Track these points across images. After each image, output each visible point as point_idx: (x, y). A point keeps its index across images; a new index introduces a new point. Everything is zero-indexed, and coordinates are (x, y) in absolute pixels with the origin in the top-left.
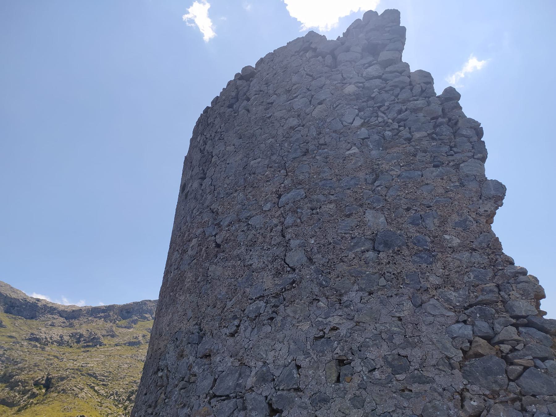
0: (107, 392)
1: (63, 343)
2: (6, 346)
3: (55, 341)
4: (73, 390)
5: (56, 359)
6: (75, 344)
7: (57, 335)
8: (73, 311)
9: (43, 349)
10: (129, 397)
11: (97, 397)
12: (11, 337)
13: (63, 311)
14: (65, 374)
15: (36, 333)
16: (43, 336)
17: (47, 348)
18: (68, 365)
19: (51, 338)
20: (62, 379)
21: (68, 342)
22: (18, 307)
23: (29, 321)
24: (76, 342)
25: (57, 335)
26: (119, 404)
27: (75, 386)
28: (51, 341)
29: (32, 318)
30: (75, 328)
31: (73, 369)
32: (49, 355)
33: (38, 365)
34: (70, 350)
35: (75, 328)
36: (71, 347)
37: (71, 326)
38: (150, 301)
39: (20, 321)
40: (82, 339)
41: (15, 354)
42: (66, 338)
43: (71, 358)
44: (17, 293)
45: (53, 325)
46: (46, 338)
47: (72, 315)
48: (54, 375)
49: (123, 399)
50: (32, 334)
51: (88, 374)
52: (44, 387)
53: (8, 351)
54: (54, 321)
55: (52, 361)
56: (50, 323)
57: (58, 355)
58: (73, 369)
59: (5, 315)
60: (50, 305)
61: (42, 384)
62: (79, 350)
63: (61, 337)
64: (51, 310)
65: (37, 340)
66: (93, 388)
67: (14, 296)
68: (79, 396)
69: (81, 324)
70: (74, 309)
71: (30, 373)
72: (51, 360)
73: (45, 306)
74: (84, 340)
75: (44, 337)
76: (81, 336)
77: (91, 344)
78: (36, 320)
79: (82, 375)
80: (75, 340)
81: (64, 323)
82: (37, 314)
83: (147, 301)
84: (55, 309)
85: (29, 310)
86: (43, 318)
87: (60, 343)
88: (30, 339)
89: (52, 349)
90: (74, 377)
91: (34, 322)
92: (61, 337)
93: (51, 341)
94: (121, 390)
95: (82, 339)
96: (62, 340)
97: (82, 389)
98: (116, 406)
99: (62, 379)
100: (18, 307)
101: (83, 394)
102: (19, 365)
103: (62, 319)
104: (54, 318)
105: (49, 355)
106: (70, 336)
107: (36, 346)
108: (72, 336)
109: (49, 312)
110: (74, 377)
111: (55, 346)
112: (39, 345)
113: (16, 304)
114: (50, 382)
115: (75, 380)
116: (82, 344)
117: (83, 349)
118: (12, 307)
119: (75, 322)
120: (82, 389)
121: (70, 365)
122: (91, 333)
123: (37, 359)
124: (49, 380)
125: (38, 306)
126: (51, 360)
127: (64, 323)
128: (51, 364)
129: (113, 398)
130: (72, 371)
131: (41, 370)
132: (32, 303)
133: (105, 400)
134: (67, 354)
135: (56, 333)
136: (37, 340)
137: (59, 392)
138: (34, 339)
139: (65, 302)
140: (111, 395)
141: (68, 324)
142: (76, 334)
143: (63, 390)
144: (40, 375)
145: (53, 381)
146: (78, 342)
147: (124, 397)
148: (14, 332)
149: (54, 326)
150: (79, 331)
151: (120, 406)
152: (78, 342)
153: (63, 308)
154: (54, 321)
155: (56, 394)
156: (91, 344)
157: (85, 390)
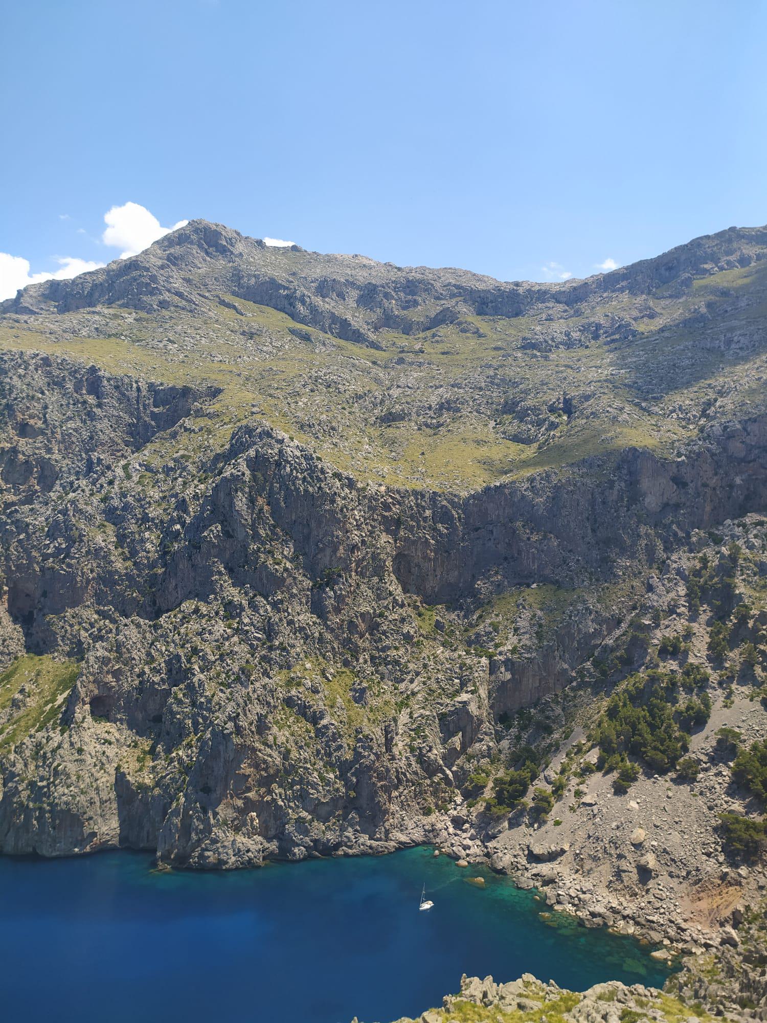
0: (663, 409)
1: (574, 344)
2: (495, 363)
3: (561, 343)
4: (608, 411)
5: (569, 370)
6: (593, 342)
7: (561, 333)
8: (575, 289)
9: (546, 358)
10: (704, 411)
11: (649, 418)
12: (497, 349)
13: (560, 293)
14: (589, 390)
15: (529, 336)
16: (541, 338)
17: (553, 356)
18: (590, 376)
19: (553, 339)
20: (587, 398)
21: (580, 341)
22: (492, 302)
23: (514, 321)
24: (593, 338)
25: (561, 333)
26: (688, 424)
27: (610, 406)
28: (554, 344)
29: (517, 315)
30: (585, 315)
31: (599, 381)
32: (557, 366)
33: (547, 384)
34: (587, 352)
35: (585, 315)
36: (587, 347)
37: (578, 313)
38: (708, 237)
39: (502, 323)
40: (602, 331)
41: (510, 373)
42: (575, 335)
43: (592, 364)
44: (485, 282)
45: (549, 319)
46: (546, 341)
47: (574, 296)
48: (573, 394)
49: (694, 416)
50: (524, 339)
51: (625, 385)
52: (565, 413)
53: (500, 370)
54: (550, 312)
55: (565, 374)
56: (544, 316)
57: (571, 363)
58: (599, 381)
59: (480, 318)
60: (536, 288)
61: (560, 409)
62: (601, 350)
63: (567, 334)
64: (541, 295)
65: (534, 346)
66: (636, 405)
67: (481, 286)
68: (620, 419)
69: (593, 308)
70: (574, 285)
71: (539, 396)
72: (562, 372)
73: (529, 291)
74: (605, 333)
75: (542, 340)
76: (598, 326)
77: (617, 337)
78: (523, 316)
79: (616, 387)
80: (590, 336)
81: (565, 311)
82: (522, 307)
83: (701, 238)
84: (545, 292)
85: (504, 303)
86: (532, 312)
87: (569, 344)
88: (523, 348)
89: (560, 356)
90: (604, 393)
91: (522, 320)
92: (567, 334)
93: (554, 344)
94: (687, 402)
95: (602, 331)
96: (569, 339)
97: (621, 409)
98: (684, 427)
99: (587, 398)
100: (492, 302)
101: (625, 416)
102: (521, 386)
103: (561, 307)
104: (549, 308)
105: (557, 366)
106: (580, 330)
107: (536, 356)
108: (584, 329)
109: (538, 299)
110: (604, 393)
111: (562, 351)
112: (538, 354)
113: (487, 298)
114: (570, 404)
115: (606, 397)
116: (602, 339)
117: (606, 348)
118: (484, 304)
119: (583, 306)
120: (621, 409)
121: (592, 375)
122: (613, 319)
123: (542, 374)
124: (567, 402)
125: (519, 294)
126: (562, 372)
127: (565, 311)
128: (565, 379)
129: (675, 416)
130: (599, 384)
131: (553, 390)
132: (510, 292)
133: (663, 420)
134: (584, 360)
135: (558, 328)
136: (534, 346)
137: (587, 418)
138: (528, 346)
139: (556, 273)
140: (672, 412)
141: (572, 312)
142: (590, 325)
143: (592, 413)
144: (553, 397)
145: (574, 402)
146: (596, 337)
147: (694, 413)
148: (498, 340)
149: (551, 320)
150: (592, 319)
151: (691, 427)
152: (596, 337)
153: (557, 288)
154: (550, 312)
155: (585, 421)
156: (617, 337)
157: (627, 409)
